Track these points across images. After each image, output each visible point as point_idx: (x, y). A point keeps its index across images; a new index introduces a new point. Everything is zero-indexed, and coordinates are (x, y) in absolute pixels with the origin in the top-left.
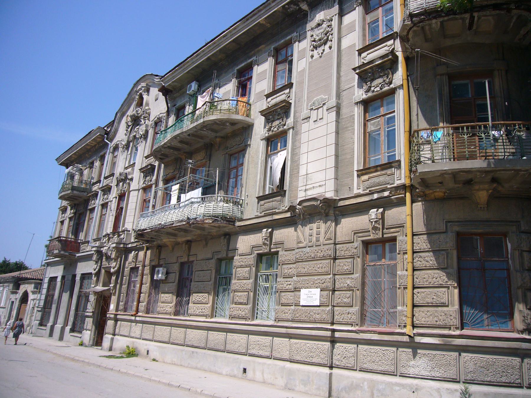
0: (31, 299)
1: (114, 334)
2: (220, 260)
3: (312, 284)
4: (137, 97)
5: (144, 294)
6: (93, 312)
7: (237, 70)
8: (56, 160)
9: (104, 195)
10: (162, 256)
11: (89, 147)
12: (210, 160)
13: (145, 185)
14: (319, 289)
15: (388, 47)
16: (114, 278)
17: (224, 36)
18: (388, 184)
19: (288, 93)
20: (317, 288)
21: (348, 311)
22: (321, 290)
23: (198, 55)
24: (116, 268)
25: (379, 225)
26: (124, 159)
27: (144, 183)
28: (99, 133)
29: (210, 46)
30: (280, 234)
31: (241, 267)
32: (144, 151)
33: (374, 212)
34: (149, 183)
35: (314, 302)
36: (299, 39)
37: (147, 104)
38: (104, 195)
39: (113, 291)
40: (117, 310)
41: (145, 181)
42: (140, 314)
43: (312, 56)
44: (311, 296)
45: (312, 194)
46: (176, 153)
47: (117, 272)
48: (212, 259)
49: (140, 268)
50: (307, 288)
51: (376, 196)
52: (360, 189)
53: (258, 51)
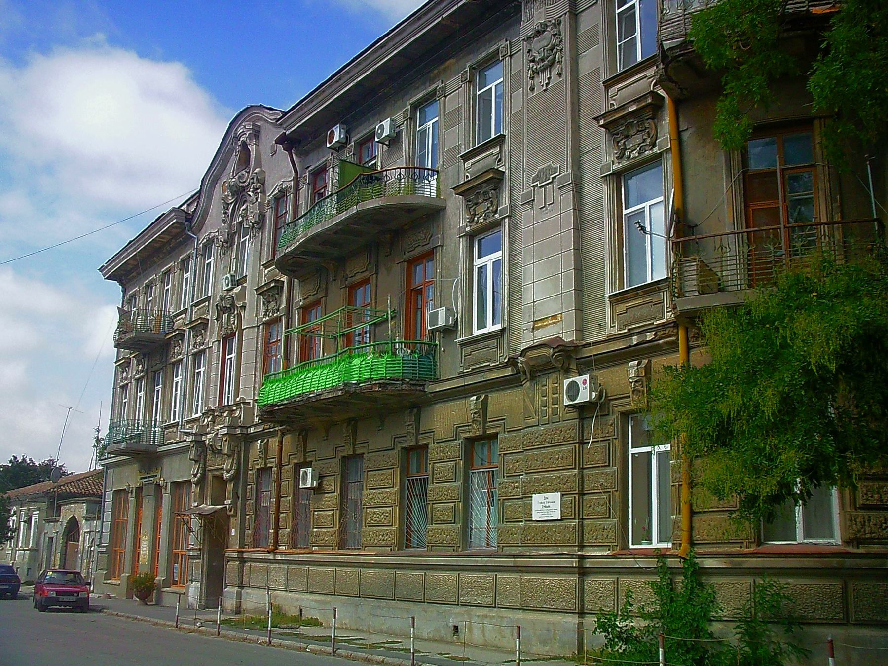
1: (241, 586)
2: (408, 450)
4: (238, 149)
5: (284, 515)
6: (200, 550)
7: (411, 104)
10: (310, 447)
11: (157, 245)
12: (377, 273)
13: (267, 318)
14: (559, 493)
15: (649, 78)
16: (230, 487)
17: (381, 47)
18: (655, 318)
19: (498, 154)
20: (556, 491)
21: (602, 527)
22: (562, 495)
23: (340, 79)
24: (232, 472)
25: (642, 387)
26: (225, 267)
27: (265, 315)
28: (175, 221)
29: (358, 64)
30: (499, 401)
31: (441, 460)
32: (261, 253)
33: (633, 367)
34: (275, 315)
36: (511, 52)
37: (258, 164)
38: (195, 337)
39: (231, 511)
40: (242, 545)
41: (267, 310)
42: (282, 548)
43: (532, 89)
44: (549, 504)
45: (544, 335)
46: (315, 260)
47: (235, 478)
48: (393, 449)
49: (273, 469)
51: (635, 340)
52: (615, 326)
53: (444, 70)
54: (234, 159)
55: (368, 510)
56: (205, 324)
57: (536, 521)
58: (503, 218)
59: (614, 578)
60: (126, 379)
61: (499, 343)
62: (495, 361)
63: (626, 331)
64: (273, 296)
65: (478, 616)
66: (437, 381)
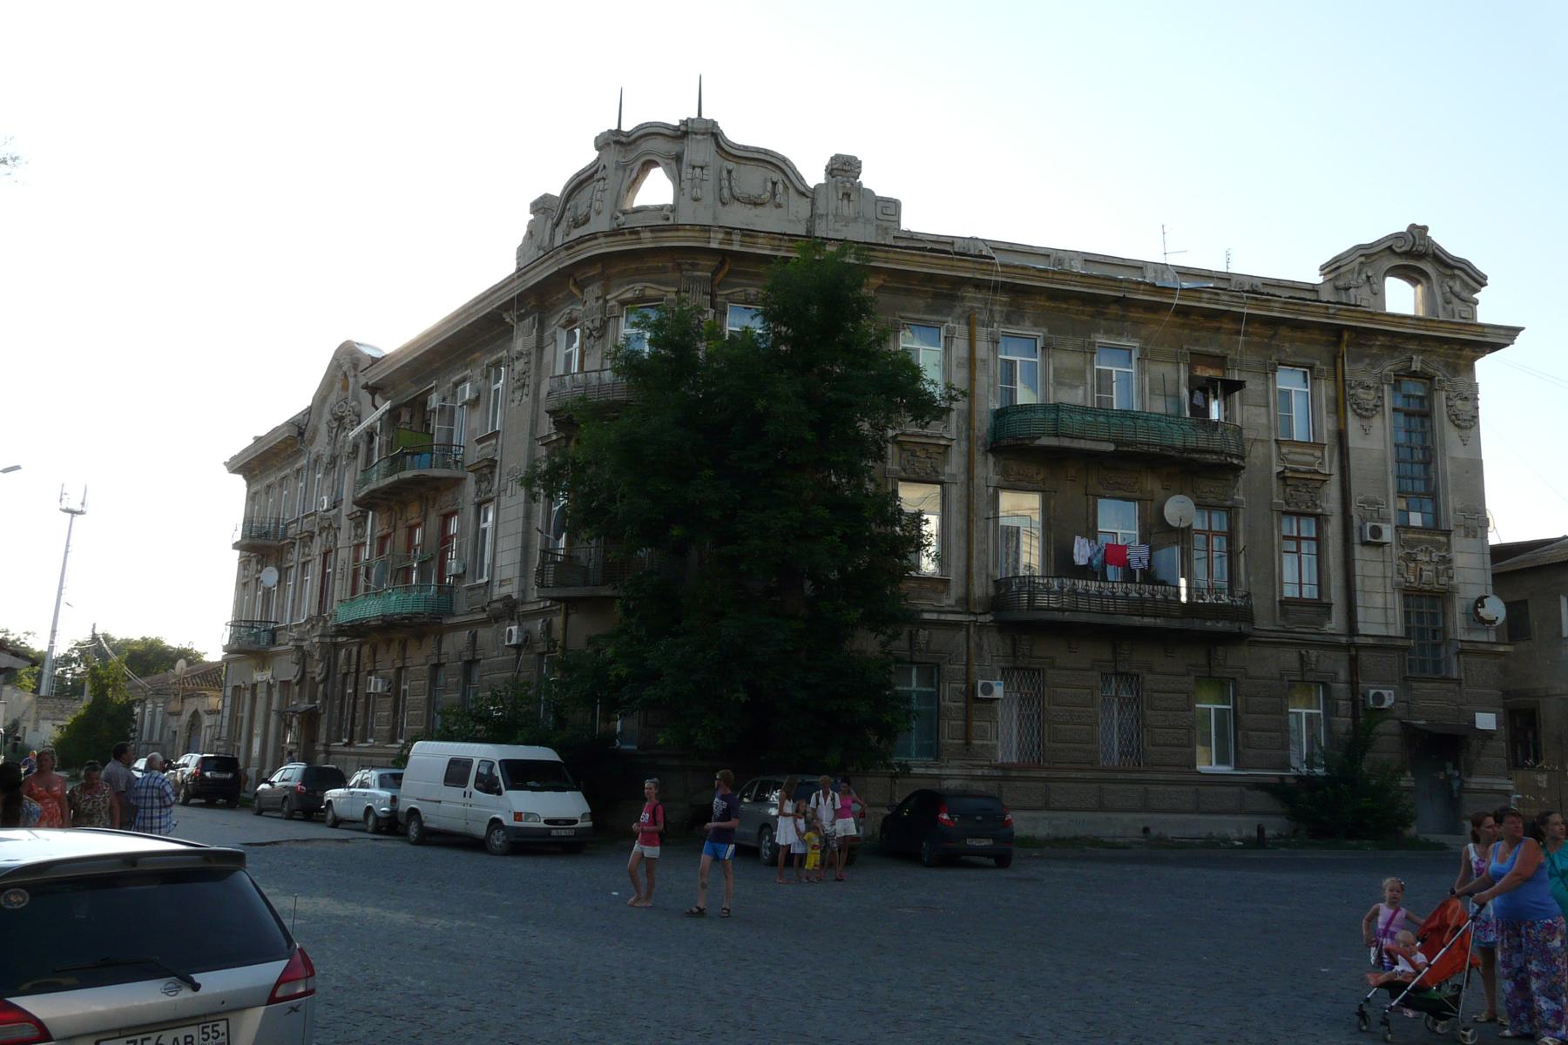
0: (207, 727)
6: (297, 743)
8: (225, 463)
9: (304, 546)
24: (322, 676)
47: (325, 680)
54: (338, 386)
55: (411, 713)
56: (312, 536)
60: (247, 577)
61: (486, 592)
64: (360, 523)
66: (453, 614)
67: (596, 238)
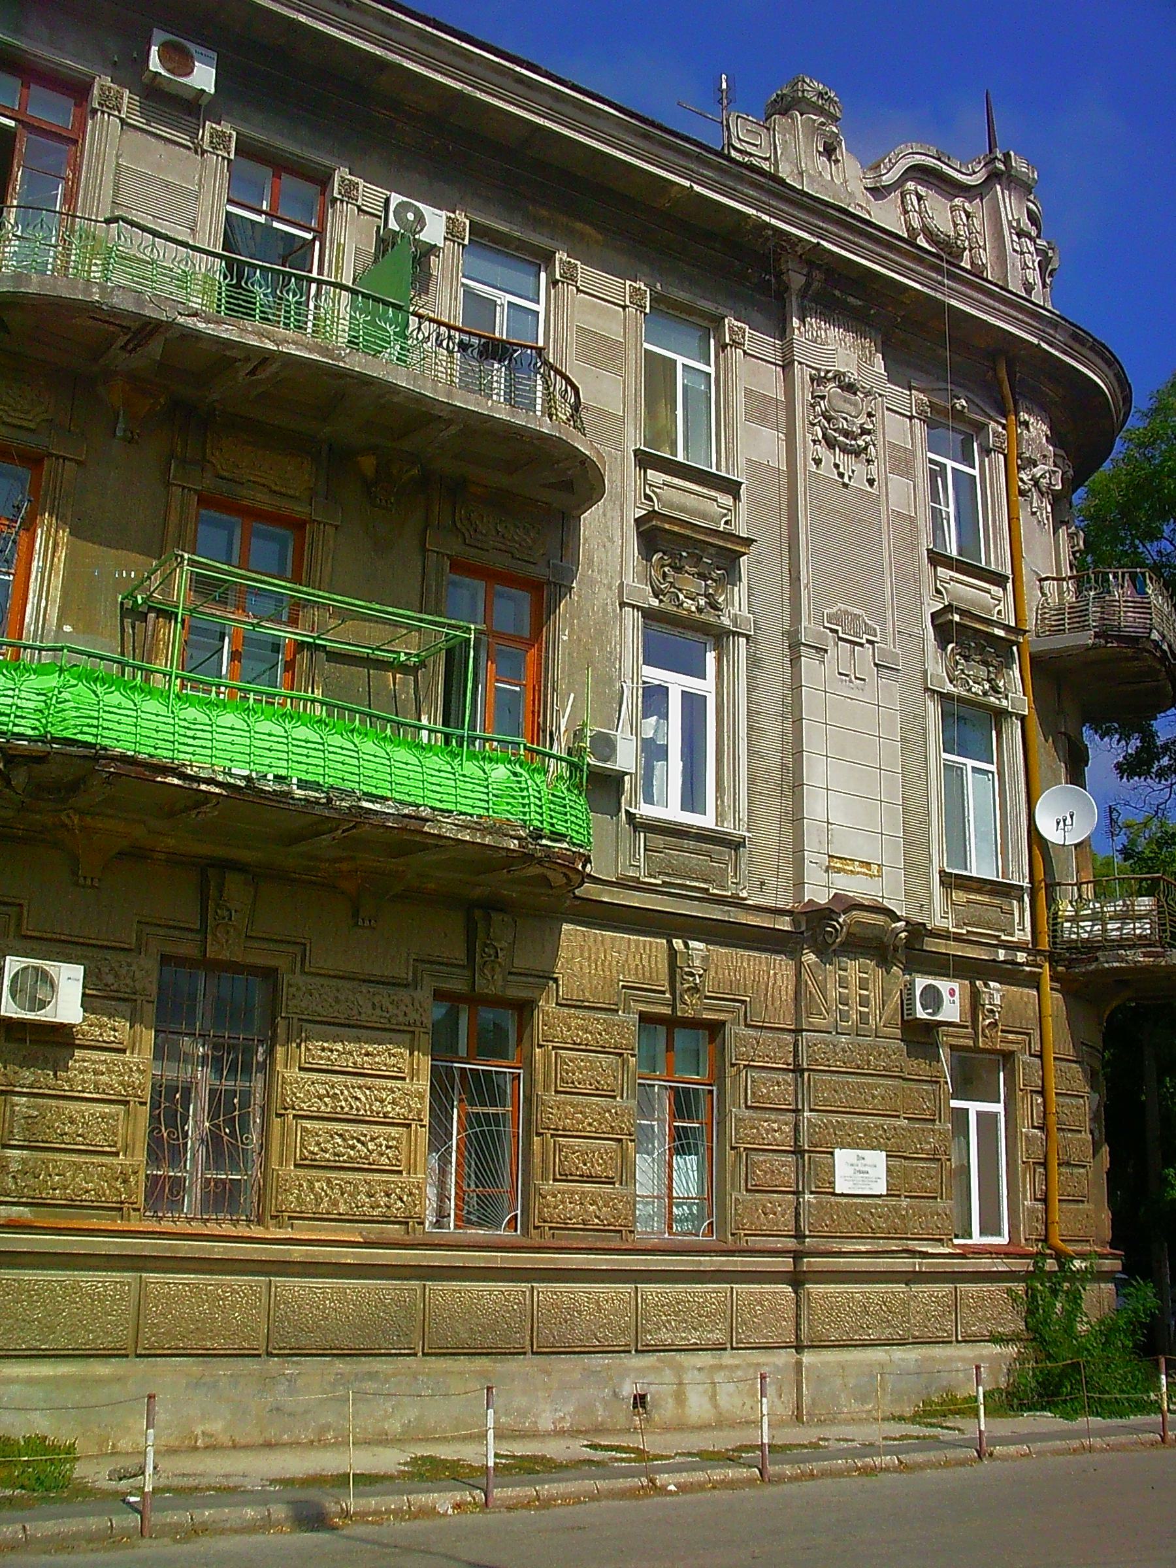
3: (860, 1138)
14: (884, 1153)
18: (1003, 931)
22: (887, 1156)
35: (873, 1185)
50: (850, 1146)
57: (842, 1195)
58: (734, 633)
59: (631, 1288)
62: (722, 887)
63: (964, 931)
65: (700, 1369)
67: (1110, 366)
